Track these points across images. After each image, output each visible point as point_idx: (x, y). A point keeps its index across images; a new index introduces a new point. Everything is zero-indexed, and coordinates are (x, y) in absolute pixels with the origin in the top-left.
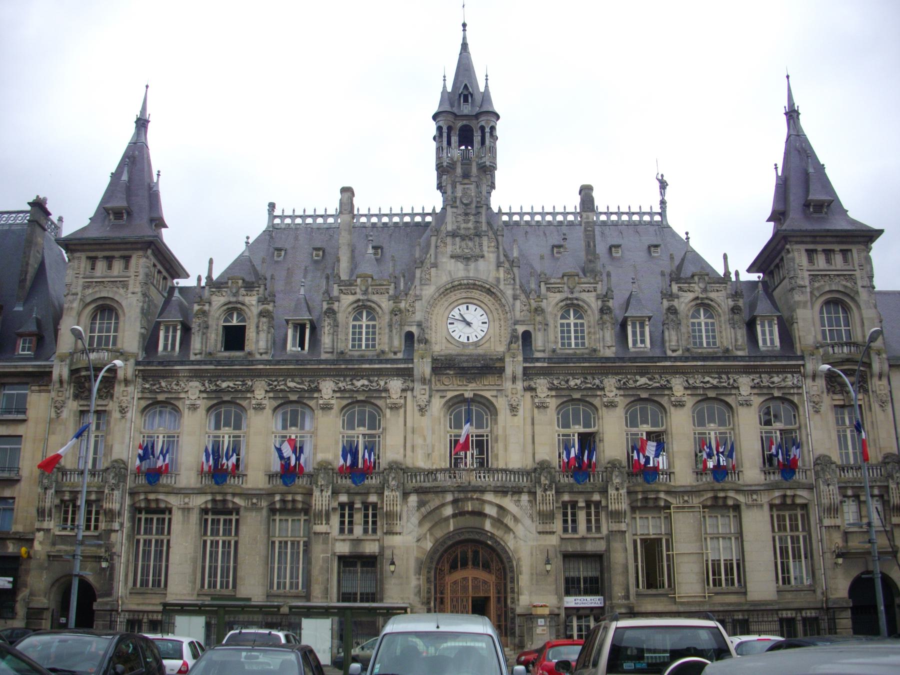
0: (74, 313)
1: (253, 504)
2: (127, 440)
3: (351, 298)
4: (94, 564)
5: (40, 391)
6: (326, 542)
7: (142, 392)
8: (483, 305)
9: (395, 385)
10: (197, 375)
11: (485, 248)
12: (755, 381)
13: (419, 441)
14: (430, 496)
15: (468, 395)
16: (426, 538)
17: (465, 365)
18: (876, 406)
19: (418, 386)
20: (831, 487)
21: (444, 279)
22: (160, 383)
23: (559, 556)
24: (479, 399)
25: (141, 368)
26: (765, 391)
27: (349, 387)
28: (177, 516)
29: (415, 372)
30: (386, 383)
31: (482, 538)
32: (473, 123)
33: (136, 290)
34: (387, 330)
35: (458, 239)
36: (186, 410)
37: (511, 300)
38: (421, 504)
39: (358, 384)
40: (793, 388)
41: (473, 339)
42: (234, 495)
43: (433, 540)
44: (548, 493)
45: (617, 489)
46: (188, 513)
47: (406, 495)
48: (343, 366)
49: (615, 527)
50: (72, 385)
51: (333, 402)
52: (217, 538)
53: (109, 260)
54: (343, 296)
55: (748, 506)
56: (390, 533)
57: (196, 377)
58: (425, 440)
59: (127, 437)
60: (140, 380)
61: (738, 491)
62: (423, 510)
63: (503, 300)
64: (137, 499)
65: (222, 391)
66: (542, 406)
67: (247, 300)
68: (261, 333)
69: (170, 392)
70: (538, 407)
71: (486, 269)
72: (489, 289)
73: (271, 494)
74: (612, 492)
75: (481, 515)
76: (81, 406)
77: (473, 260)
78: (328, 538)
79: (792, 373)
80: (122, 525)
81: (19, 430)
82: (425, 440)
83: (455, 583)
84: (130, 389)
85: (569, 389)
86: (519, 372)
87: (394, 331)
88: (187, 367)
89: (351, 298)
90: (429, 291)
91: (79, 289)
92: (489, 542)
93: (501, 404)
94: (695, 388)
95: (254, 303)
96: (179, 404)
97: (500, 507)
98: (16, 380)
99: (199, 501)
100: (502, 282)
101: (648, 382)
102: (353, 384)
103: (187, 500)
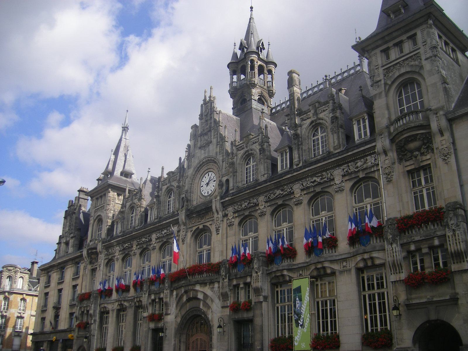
9: (175, 229)
10: (118, 243)
12: (345, 171)
16: (178, 315)
17: (198, 209)
18: (440, 162)
20: (394, 246)
23: (231, 322)
26: (353, 176)
29: (180, 220)
40: (373, 166)
44: (225, 280)
45: (257, 272)
55: (341, 272)
61: (332, 261)
75: (196, 298)
79: (370, 155)
80: (95, 321)
83: (193, 342)
93: (213, 229)
94: (308, 188)
101: (281, 193)
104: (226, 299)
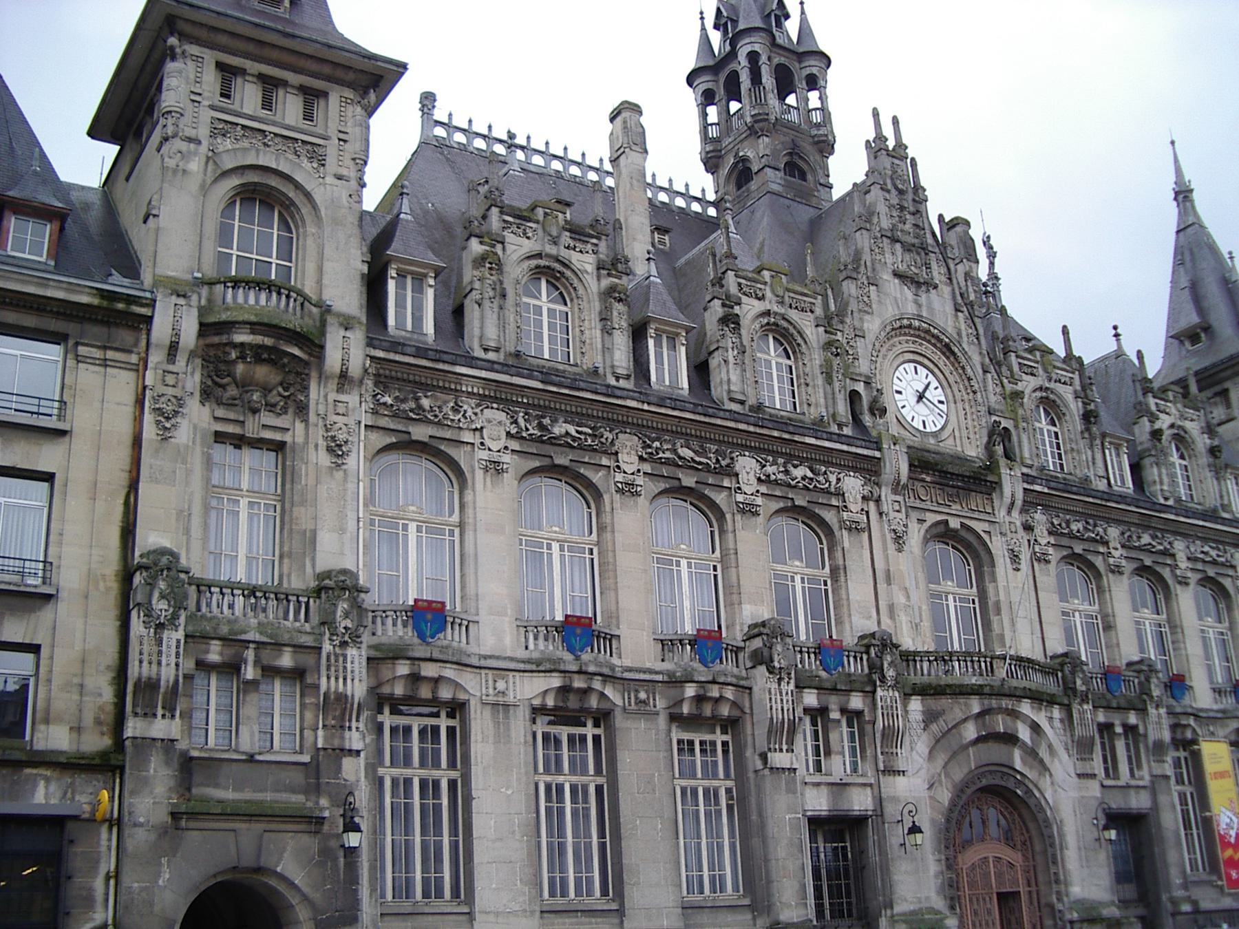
0: (193, 184)
1: (639, 702)
2: (351, 525)
3: (759, 306)
4: (306, 840)
5: (105, 363)
6: (791, 790)
7: (375, 412)
8: (936, 370)
9: (853, 485)
10: (498, 396)
11: (935, 274)
13: (900, 599)
14: (945, 702)
15: (954, 523)
16: (940, 782)
19: (886, 493)
21: (890, 312)
22: (417, 399)
24: (963, 533)
25: (381, 354)
27: (780, 476)
28: (480, 723)
30: (839, 480)
31: (1010, 784)
32: (794, 66)
33: (344, 172)
34: (820, 381)
35: (898, 246)
36: (479, 474)
37: (980, 371)
38: (930, 717)
39: (799, 472)
41: (930, 428)
42: (607, 678)
43: (950, 786)
44: (1085, 707)
45: (1157, 707)
46: (507, 717)
47: (907, 696)
48: (776, 434)
49: (1157, 771)
50: (198, 361)
51: (759, 501)
52: (561, 779)
53: (270, 85)
54: (744, 299)
56: (891, 771)
57: (495, 399)
58: (908, 597)
59: (351, 516)
60: (369, 383)
62: (934, 727)
63: (969, 370)
64: (386, 673)
65: (553, 441)
66: (1043, 559)
67: (575, 258)
68: (617, 333)
69: (439, 424)
70: (1039, 560)
71: (939, 308)
72: (947, 345)
73: (675, 681)
74: (1152, 711)
75: (1010, 739)
76: (216, 419)
77: (924, 288)
78: (794, 780)
81: (46, 457)
82: (908, 597)
83: (973, 867)
84: (352, 399)
85: (1071, 536)
86: (1020, 496)
87: (837, 385)
88: (484, 374)
89: (759, 306)
90: (872, 326)
91: (203, 132)
92: (1019, 792)
94: (1196, 560)
95: (589, 268)
96: (459, 455)
97: (1035, 728)
98: (30, 321)
99: (533, 688)
100: (965, 339)
102: (787, 472)
103: (501, 685)
104: (1087, 756)
